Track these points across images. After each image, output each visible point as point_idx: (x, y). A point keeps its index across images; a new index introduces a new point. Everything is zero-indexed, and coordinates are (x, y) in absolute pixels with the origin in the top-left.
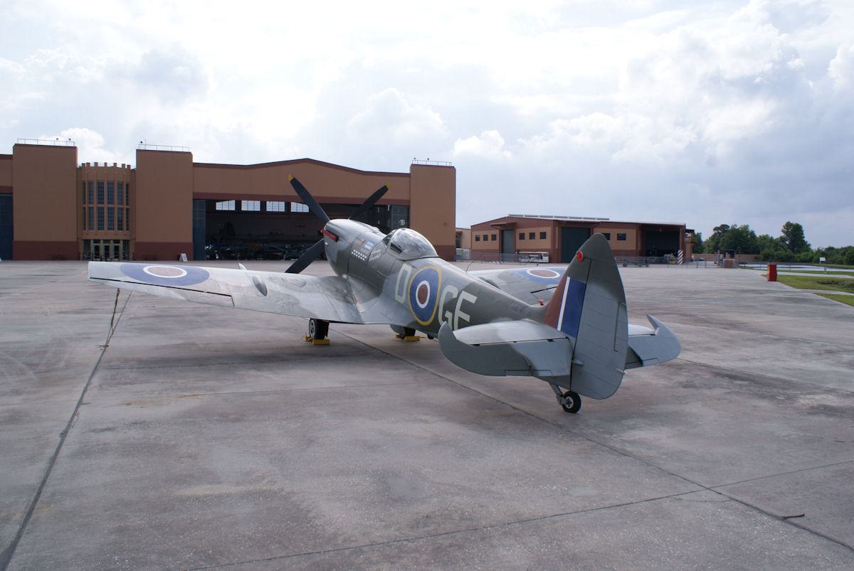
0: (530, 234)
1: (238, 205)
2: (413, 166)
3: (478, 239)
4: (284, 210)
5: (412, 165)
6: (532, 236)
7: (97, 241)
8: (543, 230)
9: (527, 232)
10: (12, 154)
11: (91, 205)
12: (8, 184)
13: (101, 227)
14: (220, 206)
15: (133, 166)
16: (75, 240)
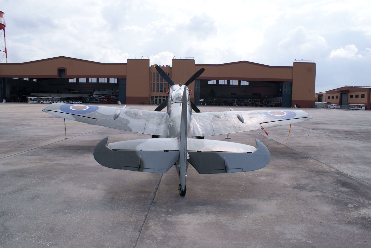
0: (362, 95)
1: (218, 82)
2: (294, 63)
3: (329, 98)
4: (227, 84)
5: (294, 63)
6: (357, 96)
7: (156, 97)
8: (363, 93)
9: (354, 94)
10: (126, 63)
11: (154, 82)
12: (125, 75)
13: (158, 91)
14: (210, 83)
15: (171, 66)
16: (148, 96)
